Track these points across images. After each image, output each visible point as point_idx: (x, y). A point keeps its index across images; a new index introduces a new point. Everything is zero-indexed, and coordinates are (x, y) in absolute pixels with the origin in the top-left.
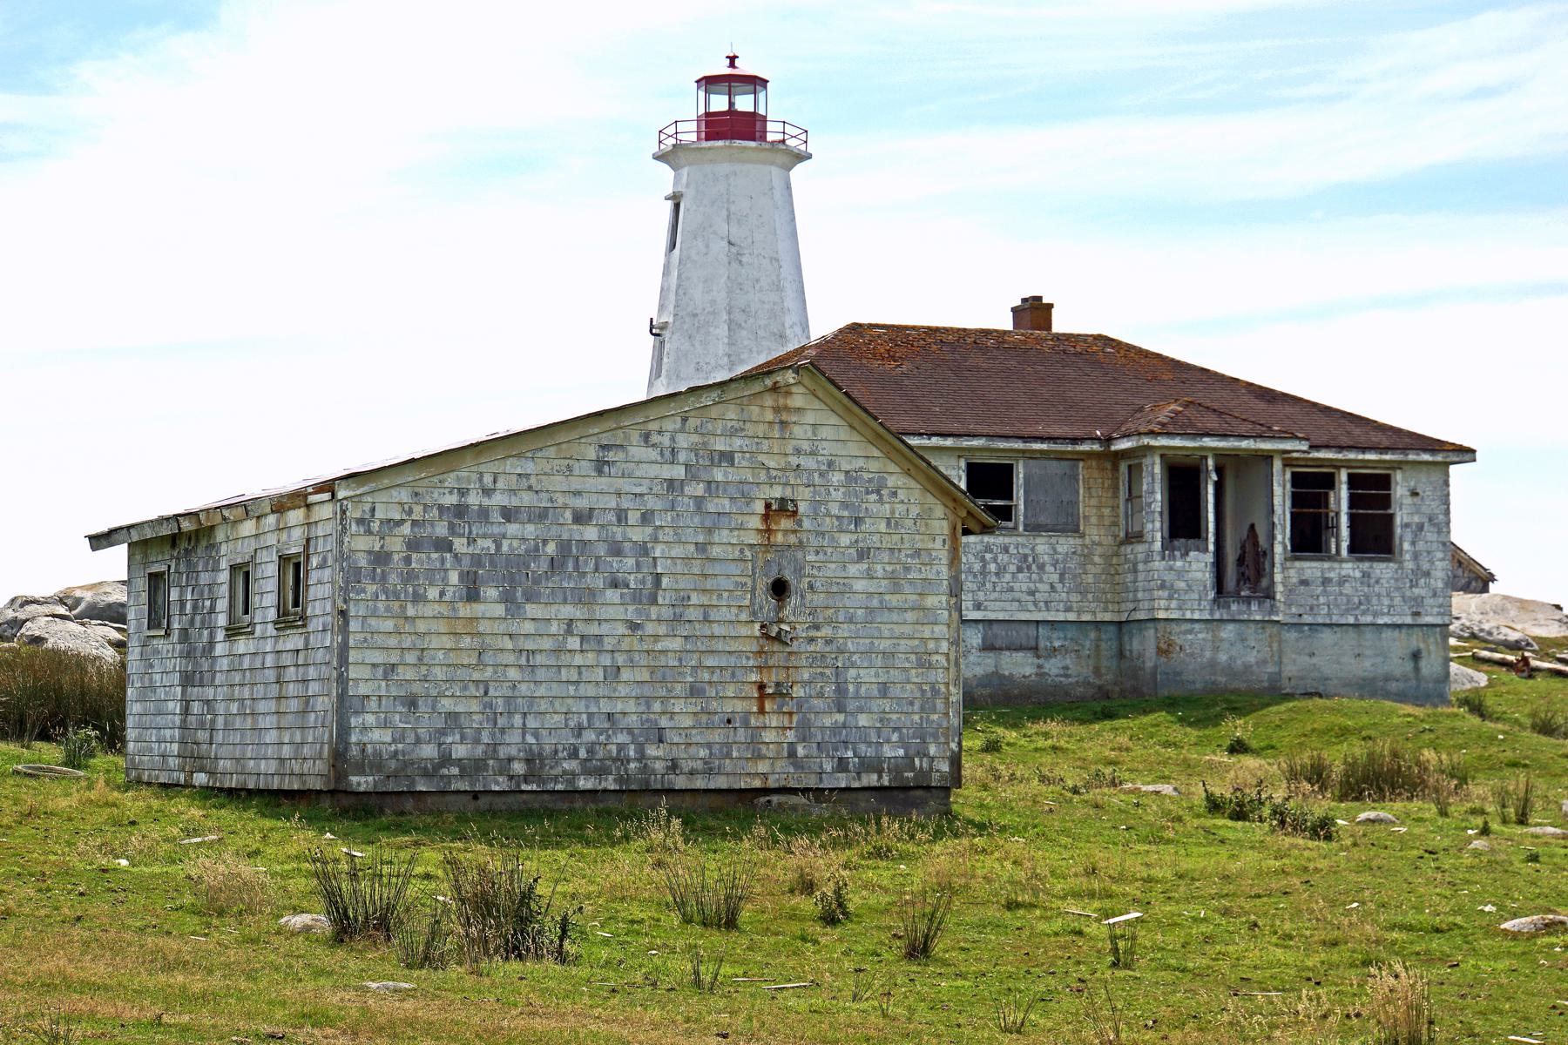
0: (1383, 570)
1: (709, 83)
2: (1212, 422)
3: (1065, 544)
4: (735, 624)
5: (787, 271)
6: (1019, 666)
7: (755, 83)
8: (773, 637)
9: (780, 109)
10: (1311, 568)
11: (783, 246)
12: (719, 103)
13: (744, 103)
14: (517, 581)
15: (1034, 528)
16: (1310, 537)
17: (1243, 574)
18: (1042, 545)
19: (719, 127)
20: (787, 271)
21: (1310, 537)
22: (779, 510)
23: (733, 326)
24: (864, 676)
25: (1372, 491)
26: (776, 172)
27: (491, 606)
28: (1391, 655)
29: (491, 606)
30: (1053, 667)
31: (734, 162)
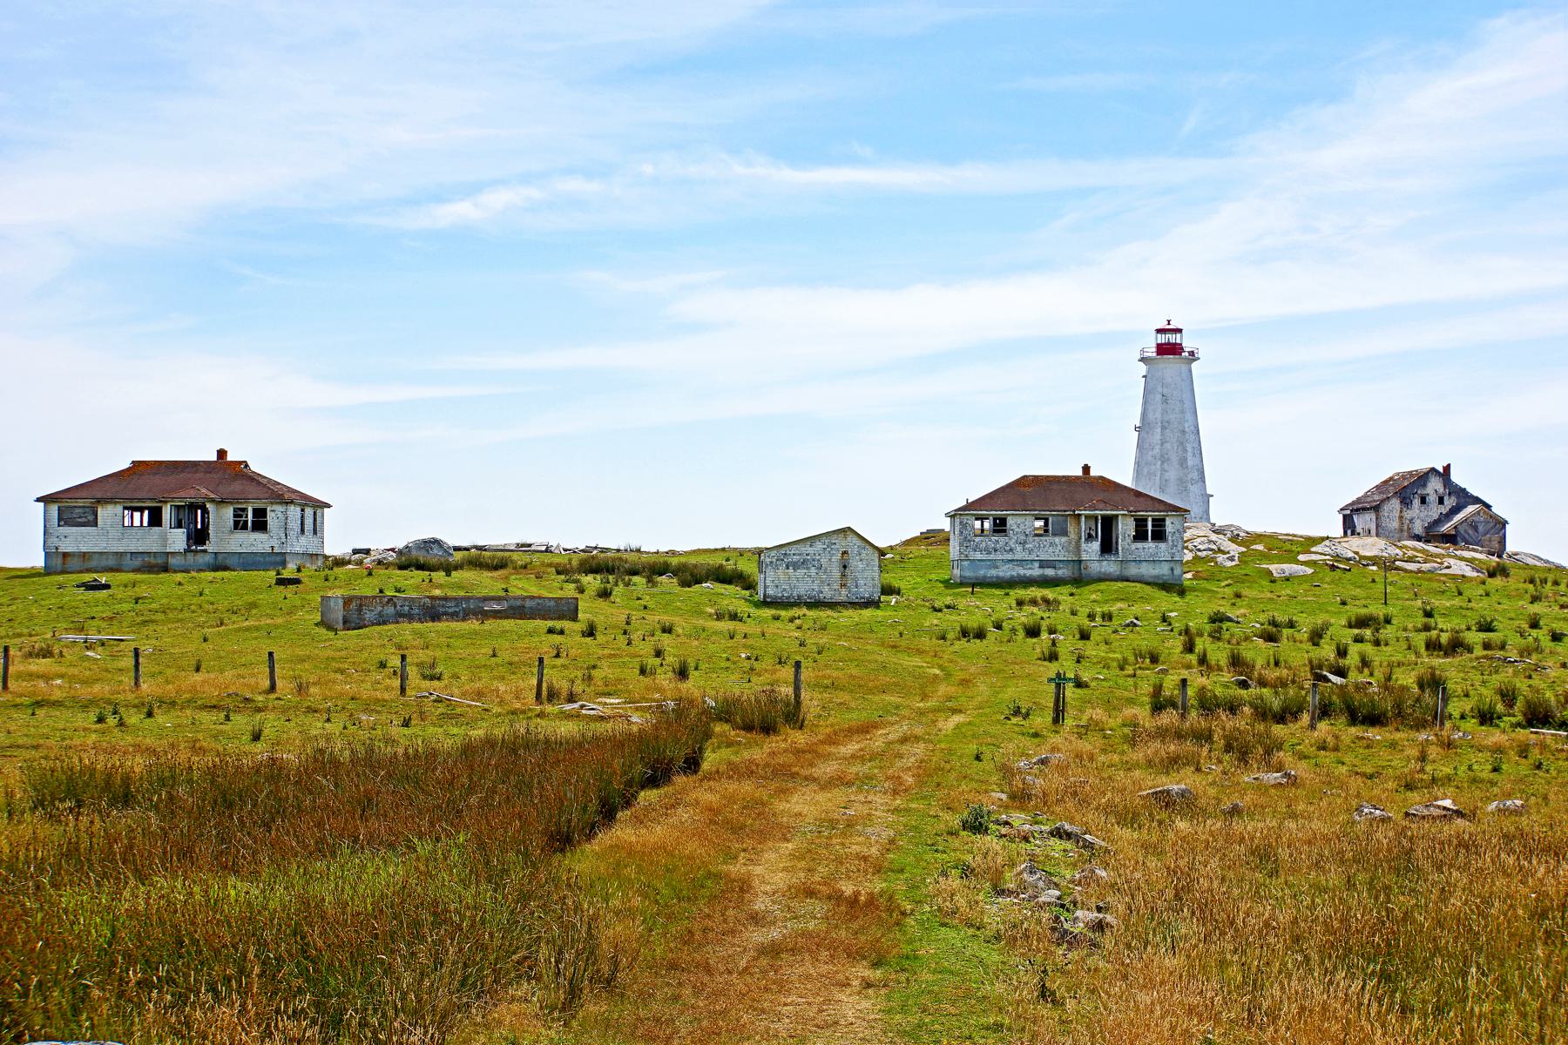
0: (1162, 545)
1: (1159, 331)
2: (1101, 505)
3: (1064, 539)
4: (836, 574)
5: (1187, 404)
6: (1050, 572)
7: (1180, 331)
8: (843, 575)
9: (1188, 345)
10: (1140, 545)
11: (1186, 396)
12: (1162, 339)
13: (1172, 338)
14: (796, 566)
15: (1054, 535)
16: (1140, 536)
17: (1108, 547)
18: (1057, 540)
19: (1163, 349)
20: (1187, 404)
21: (1140, 536)
22: (845, 553)
23: (1163, 428)
24: (861, 582)
25: (1159, 523)
26: (1184, 367)
27: (791, 570)
28: (1163, 570)
29: (791, 570)
30: (1060, 572)
31: (1170, 363)
